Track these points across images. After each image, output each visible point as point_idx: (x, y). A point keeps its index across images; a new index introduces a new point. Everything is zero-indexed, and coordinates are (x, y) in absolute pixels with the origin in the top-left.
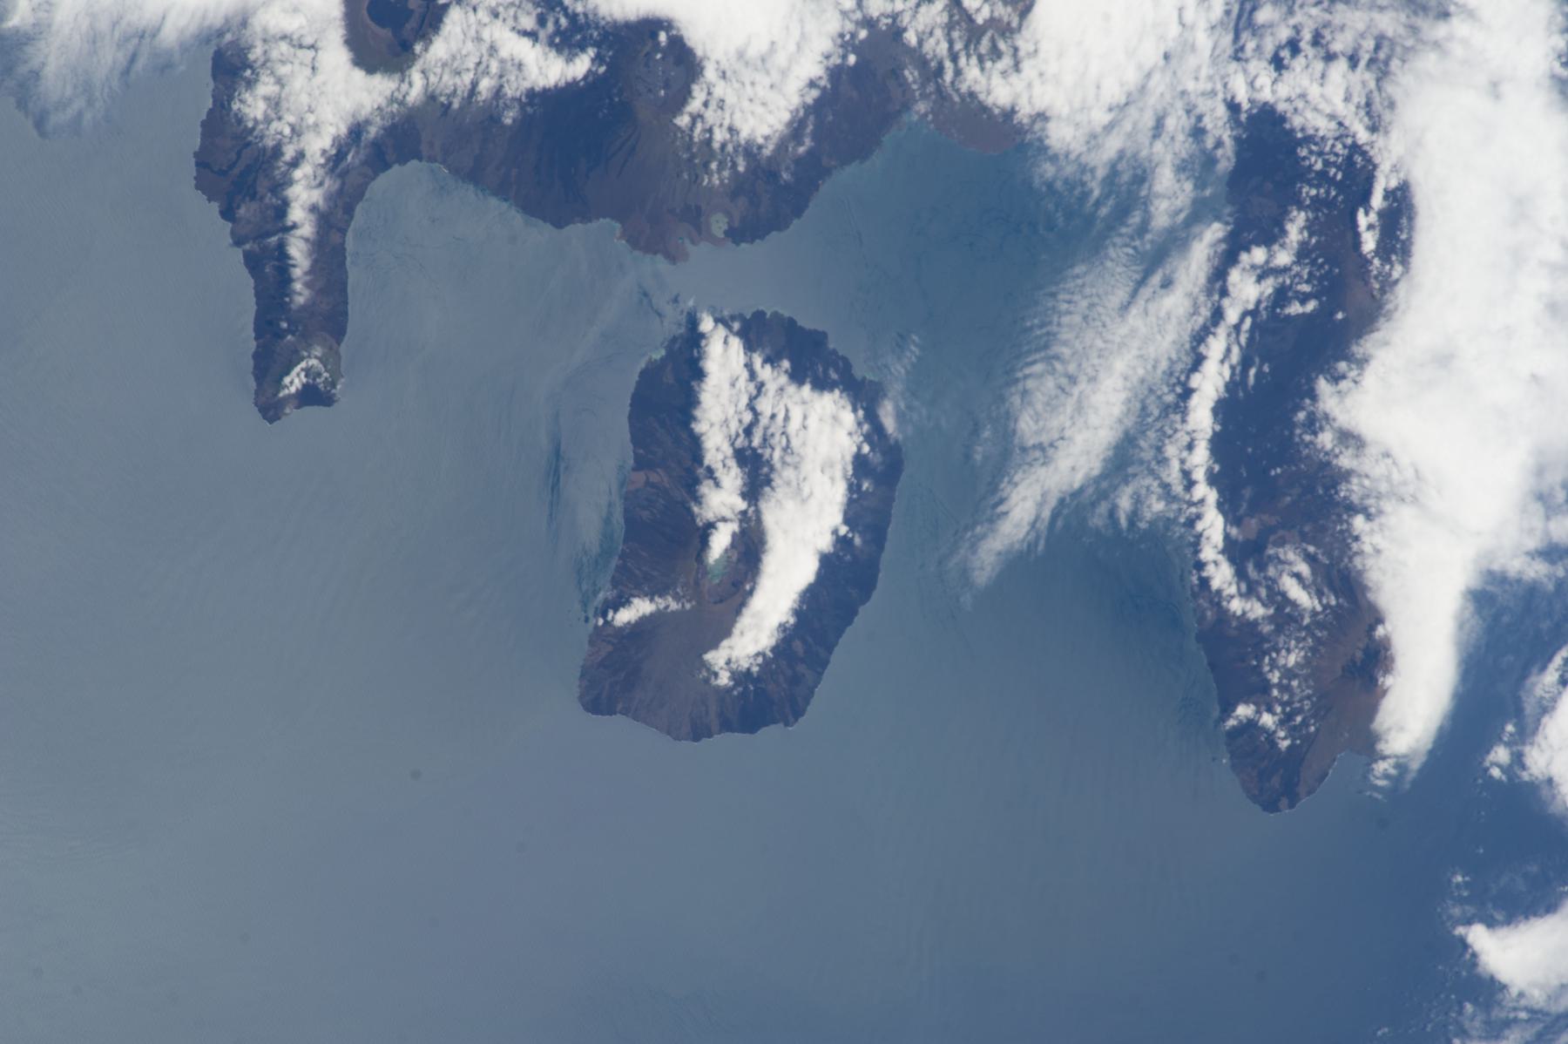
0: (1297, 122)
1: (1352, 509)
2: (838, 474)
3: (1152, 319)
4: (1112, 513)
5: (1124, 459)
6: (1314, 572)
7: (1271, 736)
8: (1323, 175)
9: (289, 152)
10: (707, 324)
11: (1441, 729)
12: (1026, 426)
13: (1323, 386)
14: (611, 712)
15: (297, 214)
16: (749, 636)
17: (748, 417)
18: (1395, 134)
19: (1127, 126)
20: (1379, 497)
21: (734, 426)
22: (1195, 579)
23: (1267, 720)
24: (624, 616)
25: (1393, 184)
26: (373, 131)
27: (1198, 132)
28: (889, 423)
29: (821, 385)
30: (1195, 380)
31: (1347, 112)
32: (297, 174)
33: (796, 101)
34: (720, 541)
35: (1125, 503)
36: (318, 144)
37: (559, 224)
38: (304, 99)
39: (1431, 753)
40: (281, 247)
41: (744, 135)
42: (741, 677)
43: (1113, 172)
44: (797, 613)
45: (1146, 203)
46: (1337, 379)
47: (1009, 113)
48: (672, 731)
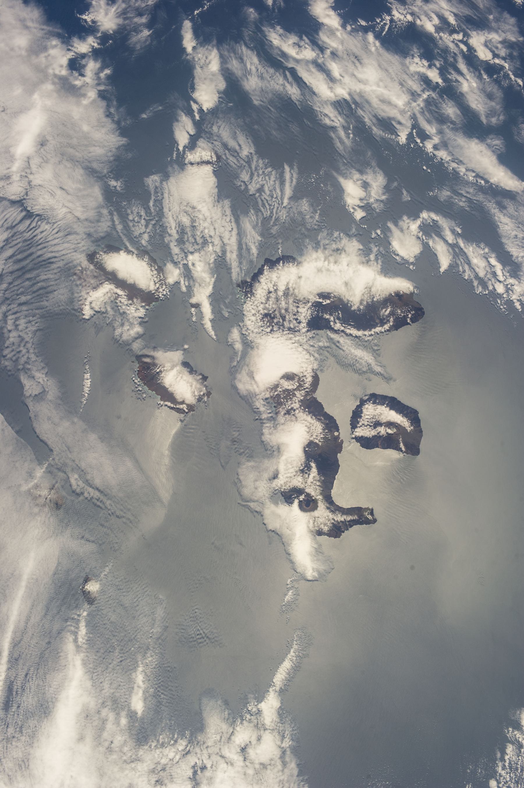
0: (309, 317)
1: (373, 301)
2: (376, 407)
3: (345, 345)
4: (377, 350)
6: (384, 308)
7: (412, 315)
8: (317, 311)
9: (333, 521)
10: (354, 436)
11: (408, 280)
13: (353, 309)
14: (419, 449)
15: (342, 519)
16: (405, 423)
17: (368, 427)
18: (310, 298)
19: (313, 352)
20: (370, 296)
21: (370, 429)
22: (387, 333)
23: (410, 316)
25: (318, 297)
26: (328, 505)
27: (313, 337)
28: (367, 397)
29: (361, 412)
30: (354, 335)
31: (306, 307)
32: (336, 520)
33: (315, 421)
34: (390, 431)
35: (376, 348)
36: (331, 516)
37: (339, 466)
38: (324, 519)
39: (412, 281)
40: (348, 522)
41: (321, 431)
42: (412, 425)
43: (320, 354)
44: (400, 414)
45: (325, 347)
46: (351, 306)
48: (421, 436)
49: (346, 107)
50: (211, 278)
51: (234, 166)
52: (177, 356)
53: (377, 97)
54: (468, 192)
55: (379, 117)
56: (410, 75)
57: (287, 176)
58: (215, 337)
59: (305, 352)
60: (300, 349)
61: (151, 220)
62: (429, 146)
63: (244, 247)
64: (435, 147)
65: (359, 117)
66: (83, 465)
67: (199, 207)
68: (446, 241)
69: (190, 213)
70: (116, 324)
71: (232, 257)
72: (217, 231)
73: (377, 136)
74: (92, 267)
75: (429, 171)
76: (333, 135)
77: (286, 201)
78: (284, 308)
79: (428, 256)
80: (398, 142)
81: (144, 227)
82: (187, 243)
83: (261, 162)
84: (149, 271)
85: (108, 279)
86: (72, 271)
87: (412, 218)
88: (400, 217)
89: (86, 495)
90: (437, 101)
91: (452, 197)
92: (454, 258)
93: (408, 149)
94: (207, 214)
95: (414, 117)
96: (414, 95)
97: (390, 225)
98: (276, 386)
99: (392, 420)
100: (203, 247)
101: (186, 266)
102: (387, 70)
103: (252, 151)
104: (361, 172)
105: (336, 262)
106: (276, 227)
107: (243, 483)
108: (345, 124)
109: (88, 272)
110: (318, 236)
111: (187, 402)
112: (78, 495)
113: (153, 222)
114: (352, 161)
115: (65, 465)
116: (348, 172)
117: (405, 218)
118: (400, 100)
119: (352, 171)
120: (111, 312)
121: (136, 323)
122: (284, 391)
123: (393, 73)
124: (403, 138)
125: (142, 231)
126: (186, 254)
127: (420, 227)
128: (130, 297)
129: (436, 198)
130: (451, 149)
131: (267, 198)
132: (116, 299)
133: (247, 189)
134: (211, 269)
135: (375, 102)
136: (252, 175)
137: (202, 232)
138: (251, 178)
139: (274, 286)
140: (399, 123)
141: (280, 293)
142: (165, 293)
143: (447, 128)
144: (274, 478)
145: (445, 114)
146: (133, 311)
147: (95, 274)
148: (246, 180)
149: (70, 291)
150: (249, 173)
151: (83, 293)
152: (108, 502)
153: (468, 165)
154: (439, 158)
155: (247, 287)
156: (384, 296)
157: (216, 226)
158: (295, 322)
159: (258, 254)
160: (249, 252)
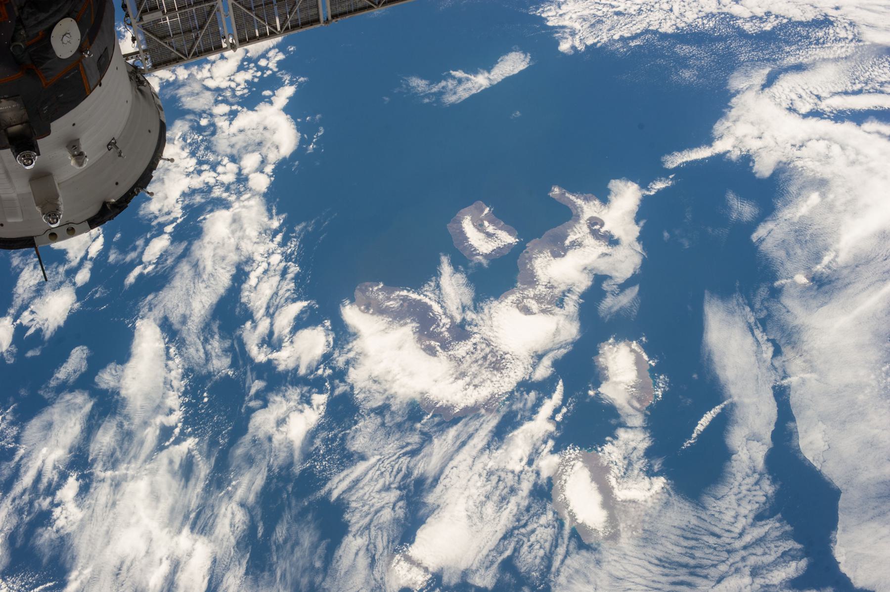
5: (438, 286)
8: (450, 343)
12: (458, 275)
23: (376, 288)
24: (488, 209)
27: (476, 325)
29: (493, 250)
31: (456, 352)
34: (486, 223)
36: (585, 208)
43: (482, 309)
47: (506, 298)
49: (200, 522)
50: (517, 436)
51: (385, 534)
52: (606, 390)
53: (157, 508)
54: (197, 350)
55: (182, 483)
56: (91, 510)
57: (344, 486)
58: (561, 383)
59: (494, 319)
60: (495, 324)
61: (523, 535)
62: (176, 418)
63: (458, 443)
64: (171, 411)
65: (202, 498)
66: (753, 359)
67: (464, 513)
68: (272, 325)
69: (478, 514)
70: (642, 453)
71: (479, 440)
72: (469, 477)
73: (210, 464)
74: (622, 526)
75: (205, 394)
76: (251, 498)
77: (373, 460)
78: (475, 365)
79: (300, 323)
80: (198, 444)
81: (537, 532)
82: (509, 485)
83: (354, 520)
84: (569, 482)
85: (615, 500)
86: (644, 536)
87: (276, 362)
88: (287, 372)
89: (765, 338)
90: (105, 458)
91: (217, 356)
92: (282, 306)
93: (197, 430)
94: (462, 500)
95: (150, 458)
96: (117, 485)
97: (302, 371)
98: (544, 311)
99: (475, 230)
100: (497, 470)
101: (530, 462)
102: (107, 532)
103: (350, 537)
104: (270, 439)
105: (389, 372)
106: (409, 441)
107: (633, 266)
108: (226, 499)
109: (629, 523)
110: (379, 407)
111: (628, 349)
112: (773, 342)
113: (523, 530)
114: (265, 456)
115: (768, 369)
116: (282, 446)
117: (281, 368)
118: (138, 488)
119: (277, 446)
120: (638, 466)
121: (621, 443)
122: (541, 303)
123: (106, 524)
124: (190, 443)
125: (542, 530)
126: (519, 476)
127: (277, 351)
128: (607, 469)
129: (234, 365)
130: (158, 401)
131: (387, 474)
132: (622, 477)
133: (400, 498)
134: (509, 444)
135: (165, 505)
136: (377, 512)
137: (485, 486)
138: (383, 507)
139: (466, 389)
140: (171, 462)
141: (467, 379)
142: (572, 451)
143: (132, 424)
144: (606, 254)
145: (117, 441)
146: (615, 454)
147: (623, 516)
148: (389, 510)
149: (659, 516)
150: (379, 514)
151: (650, 504)
152: (752, 320)
153: (164, 374)
154: (180, 401)
155: (489, 405)
156: (380, 317)
157: (464, 482)
158: (478, 347)
159: (452, 426)
160: (458, 435)
